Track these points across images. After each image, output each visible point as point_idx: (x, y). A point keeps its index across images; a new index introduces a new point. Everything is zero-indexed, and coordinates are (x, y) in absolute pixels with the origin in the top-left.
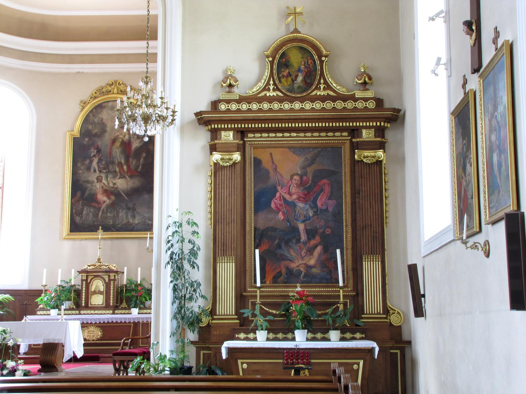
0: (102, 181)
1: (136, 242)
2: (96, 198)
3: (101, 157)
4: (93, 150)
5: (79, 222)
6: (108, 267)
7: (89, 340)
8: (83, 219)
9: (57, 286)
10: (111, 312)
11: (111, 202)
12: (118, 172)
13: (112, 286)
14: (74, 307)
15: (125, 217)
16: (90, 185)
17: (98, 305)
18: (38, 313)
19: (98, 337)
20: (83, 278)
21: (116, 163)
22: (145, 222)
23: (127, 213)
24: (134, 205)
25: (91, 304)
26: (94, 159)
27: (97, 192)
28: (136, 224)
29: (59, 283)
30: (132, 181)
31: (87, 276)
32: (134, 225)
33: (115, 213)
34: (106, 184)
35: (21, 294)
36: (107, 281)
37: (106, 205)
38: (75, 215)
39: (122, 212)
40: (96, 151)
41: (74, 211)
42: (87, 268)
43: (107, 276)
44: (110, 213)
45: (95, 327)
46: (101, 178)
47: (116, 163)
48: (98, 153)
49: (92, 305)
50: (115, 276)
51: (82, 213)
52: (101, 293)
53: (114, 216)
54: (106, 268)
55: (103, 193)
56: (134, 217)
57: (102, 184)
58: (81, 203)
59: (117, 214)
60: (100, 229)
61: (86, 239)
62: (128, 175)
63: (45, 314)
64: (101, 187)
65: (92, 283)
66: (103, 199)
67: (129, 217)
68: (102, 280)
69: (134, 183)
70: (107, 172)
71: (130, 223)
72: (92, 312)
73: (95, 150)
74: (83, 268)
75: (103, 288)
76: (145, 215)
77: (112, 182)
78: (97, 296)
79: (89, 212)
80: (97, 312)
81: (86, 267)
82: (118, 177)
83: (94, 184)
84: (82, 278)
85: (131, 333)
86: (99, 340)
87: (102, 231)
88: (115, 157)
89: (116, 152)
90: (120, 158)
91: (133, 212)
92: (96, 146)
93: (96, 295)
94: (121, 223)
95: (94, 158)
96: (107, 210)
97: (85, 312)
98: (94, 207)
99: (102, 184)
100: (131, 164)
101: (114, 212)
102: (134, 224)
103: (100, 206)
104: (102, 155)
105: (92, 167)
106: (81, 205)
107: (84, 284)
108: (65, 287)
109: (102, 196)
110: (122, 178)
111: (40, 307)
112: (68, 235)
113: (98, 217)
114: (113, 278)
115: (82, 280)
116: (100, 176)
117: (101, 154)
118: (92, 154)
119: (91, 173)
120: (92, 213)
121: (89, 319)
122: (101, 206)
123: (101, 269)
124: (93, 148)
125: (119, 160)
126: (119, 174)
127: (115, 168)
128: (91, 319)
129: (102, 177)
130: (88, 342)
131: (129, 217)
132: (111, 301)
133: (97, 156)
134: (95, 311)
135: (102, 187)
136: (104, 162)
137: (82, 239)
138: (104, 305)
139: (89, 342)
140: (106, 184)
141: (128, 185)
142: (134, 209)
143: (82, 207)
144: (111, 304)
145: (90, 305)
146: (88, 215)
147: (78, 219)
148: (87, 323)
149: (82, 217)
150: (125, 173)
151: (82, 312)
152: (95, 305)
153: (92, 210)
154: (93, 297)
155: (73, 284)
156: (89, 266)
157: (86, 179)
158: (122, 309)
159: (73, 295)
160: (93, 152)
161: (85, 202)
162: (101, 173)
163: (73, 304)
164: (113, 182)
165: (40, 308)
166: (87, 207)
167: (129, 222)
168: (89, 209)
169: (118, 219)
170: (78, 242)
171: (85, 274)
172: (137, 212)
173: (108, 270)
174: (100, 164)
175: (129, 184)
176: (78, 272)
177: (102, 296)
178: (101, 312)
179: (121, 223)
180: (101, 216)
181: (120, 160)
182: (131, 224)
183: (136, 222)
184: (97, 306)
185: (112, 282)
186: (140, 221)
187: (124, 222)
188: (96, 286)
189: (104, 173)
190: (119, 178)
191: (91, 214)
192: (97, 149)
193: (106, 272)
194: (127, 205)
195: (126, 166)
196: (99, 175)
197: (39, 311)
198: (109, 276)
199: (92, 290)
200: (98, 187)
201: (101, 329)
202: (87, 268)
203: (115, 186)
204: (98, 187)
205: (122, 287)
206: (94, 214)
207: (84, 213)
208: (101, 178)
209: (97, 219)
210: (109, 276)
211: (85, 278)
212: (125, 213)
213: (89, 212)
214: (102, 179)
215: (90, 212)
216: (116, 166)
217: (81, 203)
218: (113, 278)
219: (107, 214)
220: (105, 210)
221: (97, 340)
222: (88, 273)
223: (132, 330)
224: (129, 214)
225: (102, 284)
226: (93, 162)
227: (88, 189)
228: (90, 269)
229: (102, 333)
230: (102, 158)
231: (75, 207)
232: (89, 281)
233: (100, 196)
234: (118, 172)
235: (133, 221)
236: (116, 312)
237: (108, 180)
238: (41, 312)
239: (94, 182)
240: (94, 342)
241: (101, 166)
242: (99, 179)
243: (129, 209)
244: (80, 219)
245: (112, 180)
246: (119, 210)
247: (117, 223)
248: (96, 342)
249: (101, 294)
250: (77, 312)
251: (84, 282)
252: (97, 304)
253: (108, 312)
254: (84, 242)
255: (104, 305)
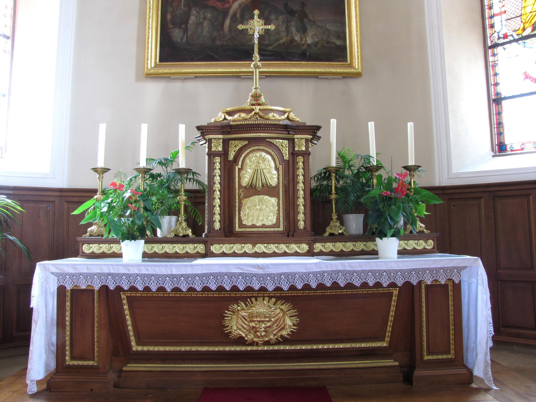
1: (309, 85)
5: (179, 40)
6: (286, 116)
7: (252, 343)
8: (189, 33)
9: (139, 170)
10: (305, 247)
13: (301, 172)
14: (189, 232)
15: (284, 29)
17: (264, 226)
18: (86, 249)
19: (284, 333)
20: (213, 149)
22: (328, 42)
23: (287, 23)
24: (303, 5)
25: (241, 225)
28: (309, 45)
29: (143, 164)
31: (226, 143)
32: (305, 47)
35: (51, 199)
36: (286, 157)
37: (240, 5)
38: (170, 26)
39: (277, 19)
41: (169, 17)
42: (225, 119)
43: (286, 142)
45: (273, 300)
49: (245, 226)
50: (307, 140)
51: (186, 23)
52: (270, 191)
54: (283, 117)
56: (303, 30)
60: (256, 17)
61: (198, 77)
63: (106, 251)
65: (246, 156)
67: (293, 29)
68: (273, 153)
71: (295, 44)
72: (248, 248)
74: (213, 121)
75: (275, 177)
76: (328, 28)
78: (260, 201)
79: (201, 20)
80: (261, 248)
81: (220, 116)
84: (210, 147)
85: (391, 318)
86: (285, 341)
87: (262, 22)
91: (302, 21)
93: (256, 198)
97: (226, 248)
98: (214, 8)
102: (303, 44)
103: (226, 6)
106: (185, 6)
107: (218, 166)
108: (160, 175)
111: (91, 231)
112: (156, 66)
113: (223, 29)
114: (304, 149)
115: (211, 155)
120: (210, 20)
121: (254, 275)
122: (230, 7)
123: (268, 119)
128: (262, 276)
130: (249, 348)
131: (293, 29)
132: (301, 217)
134: (254, 246)
137: (186, 77)
138: (281, 229)
139: (255, 348)
142: (303, 16)
143: (186, 9)
144: (301, 224)
145: (237, 229)
146: (199, 24)
147: (177, 34)
148: (249, 289)
149: (186, 30)
151: (215, 248)
152: (254, 226)
154: (249, 204)
155: (182, 164)
156: (230, 113)
158: (333, 238)
159: (184, 198)
163: (184, 224)
165: (91, 235)
166: (198, 9)
167: (292, 41)
168: (203, 14)
170: (177, 86)
171: (221, 136)
172: (310, 20)
173: (287, 122)
176: (199, 128)
177: (274, 200)
178: (272, 248)
180: (230, 26)
182: (299, 45)
183: (309, 41)
184: (260, 229)
185: (300, 159)
186: (316, 40)
187: (281, 41)
188: (256, 171)
191: (206, 24)
193: (286, 128)
194: (286, 5)
197: (89, 242)
198: (292, 141)
199: (246, 181)
201: (293, 308)
202: (225, 119)
205: (326, 174)
207: (190, 22)
209: (222, 32)
210: (292, 141)
211: (220, 149)
212: (283, 22)
213: (201, 20)
215: (205, 18)
218: (304, 149)
220: (238, 15)
221: (278, 343)
222: (229, 133)
223: (393, 308)
224: (293, 23)
225: (272, 164)
228: (234, 121)
229: (296, 320)
231: (170, 9)
232: (231, 157)
236: (318, 247)
238: (95, 248)
240: (271, 348)
243: (291, 13)
244: (182, 34)
247: (267, 42)
248: (276, 348)
249: (271, 196)
250: (201, 248)
251: (218, 160)
252: (259, 224)
253: (294, 247)
254: (191, 86)
255: (281, 229)
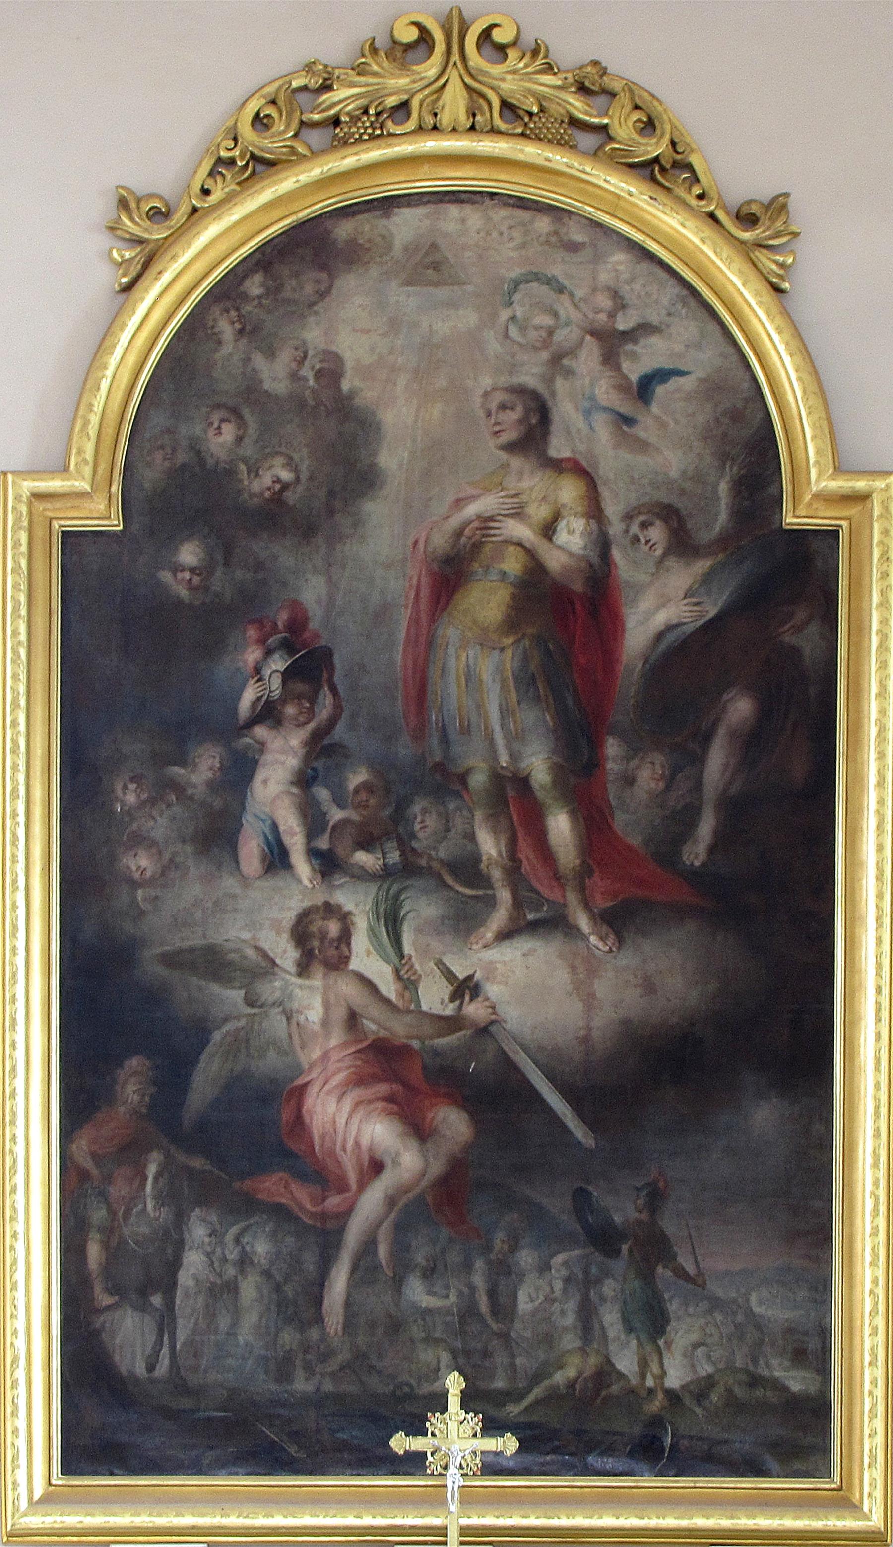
0: (345, 959)
2: (299, 1122)
3: (332, 723)
4: (253, 655)
11: (437, 1168)
12: (496, 874)
15: (570, 1319)
16: (236, 996)
21: (479, 780)
26: (262, 746)
27: (298, 1070)
30: (627, 959)
32: (656, 1405)
33: (479, 1280)
34: (389, 988)
37: (391, 1201)
39: (544, 1268)
40: (278, 664)
44: (429, 1274)
46: (333, 928)
47: (479, 780)
48: (300, 687)
53: (469, 1312)
55: (359, 1080)
57: (348, 989)
58: (152, 1170)
59: (492, 1294)
62: (587, 905)
64: (339, 1014)
66: (365, 1142)
69: (649, 987)
70: (387, 874)
71: (615, 1389)
73: (269, 653)
77: (440, 963)
79: (231, 1271)
82: (499, 918)
83: (270, 990)
88: (466, 730)
89: (471, 677)
90: (515, 738)
92: (282, 618)
94: (536, 1378)
95: (260, 731)
96: (400, 1248)
99: (348, 989)
100: (612, 792)
101: (467, 1266)
103: (334, 1202)
104: (338, 709)
105: (248, 819)
109: (347, 1104)
110: (533, 928)
113: (319, 1319)
116: (330, 910)
117: (326, 700)
118: (249, 696)
119: (245, 882)
124: (252, 633)
125: (504, 760)
126: (504, 896)
127: (471, 837)
129: (345, 918)
133: (290, 710)
135: (353, 1019)
136: (357, 777)
140: (389, 988)
141: (590, 1001)
143: (165, 1215)
150: (557, 877)
153: (261, 1248)
157: (194, 940)
160: (257, 670)
161: (198, 1163)
162: (339, 879)
164: (449, 975)
168: (237, 1240)
169: (504, 1337)
174: (323, 794)
175: (602, 988)
179: (536, 1378)
180: (348, 1304)
181: (514, 757)
183: (675, 1378)
189: (362, 875)
190: (505, 936)
192: (288, 647)
194: (581, 1198)
195: (573, 814)
196: (319, 899)
200: (314, 1014)
203: (474, 1010)
204: (314, 1014)
206: (278, 1288)
207: (185, 1279)
208: (333, 928)
209: (314, 1334)
214: (346, 936)
216: (479, 815)
217: (152, 1170)
219: (398, 1283)
226: (261, 775)
227: (217, 1036)
230: (340, 732)
231: (98, 1215)
233: (332, 1107)
234: (496, 874)
235: (644, 1365)
237: (407, 949)
239: (271, 964)
241: (336, 815)
242: (323, 935)
245: (436, 945)
246: (514, 1248)
247: (499, 1384)
